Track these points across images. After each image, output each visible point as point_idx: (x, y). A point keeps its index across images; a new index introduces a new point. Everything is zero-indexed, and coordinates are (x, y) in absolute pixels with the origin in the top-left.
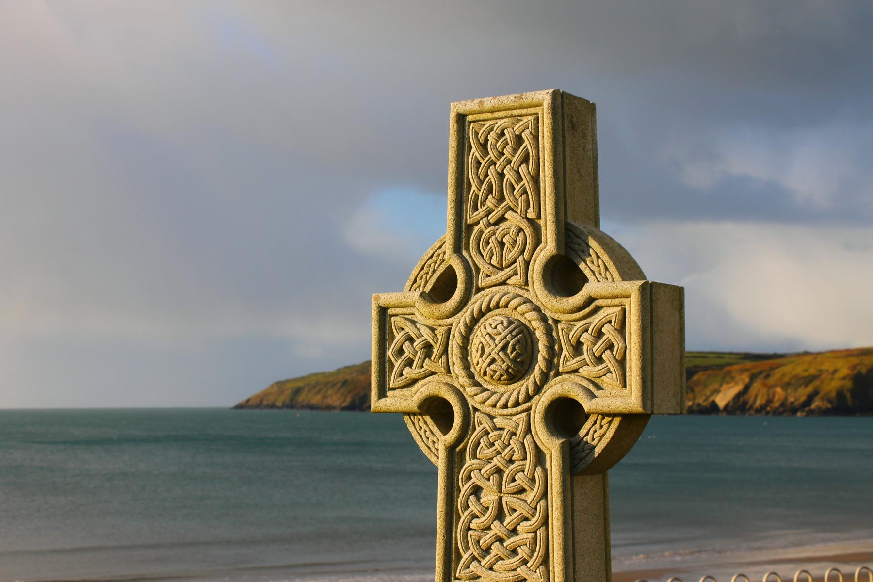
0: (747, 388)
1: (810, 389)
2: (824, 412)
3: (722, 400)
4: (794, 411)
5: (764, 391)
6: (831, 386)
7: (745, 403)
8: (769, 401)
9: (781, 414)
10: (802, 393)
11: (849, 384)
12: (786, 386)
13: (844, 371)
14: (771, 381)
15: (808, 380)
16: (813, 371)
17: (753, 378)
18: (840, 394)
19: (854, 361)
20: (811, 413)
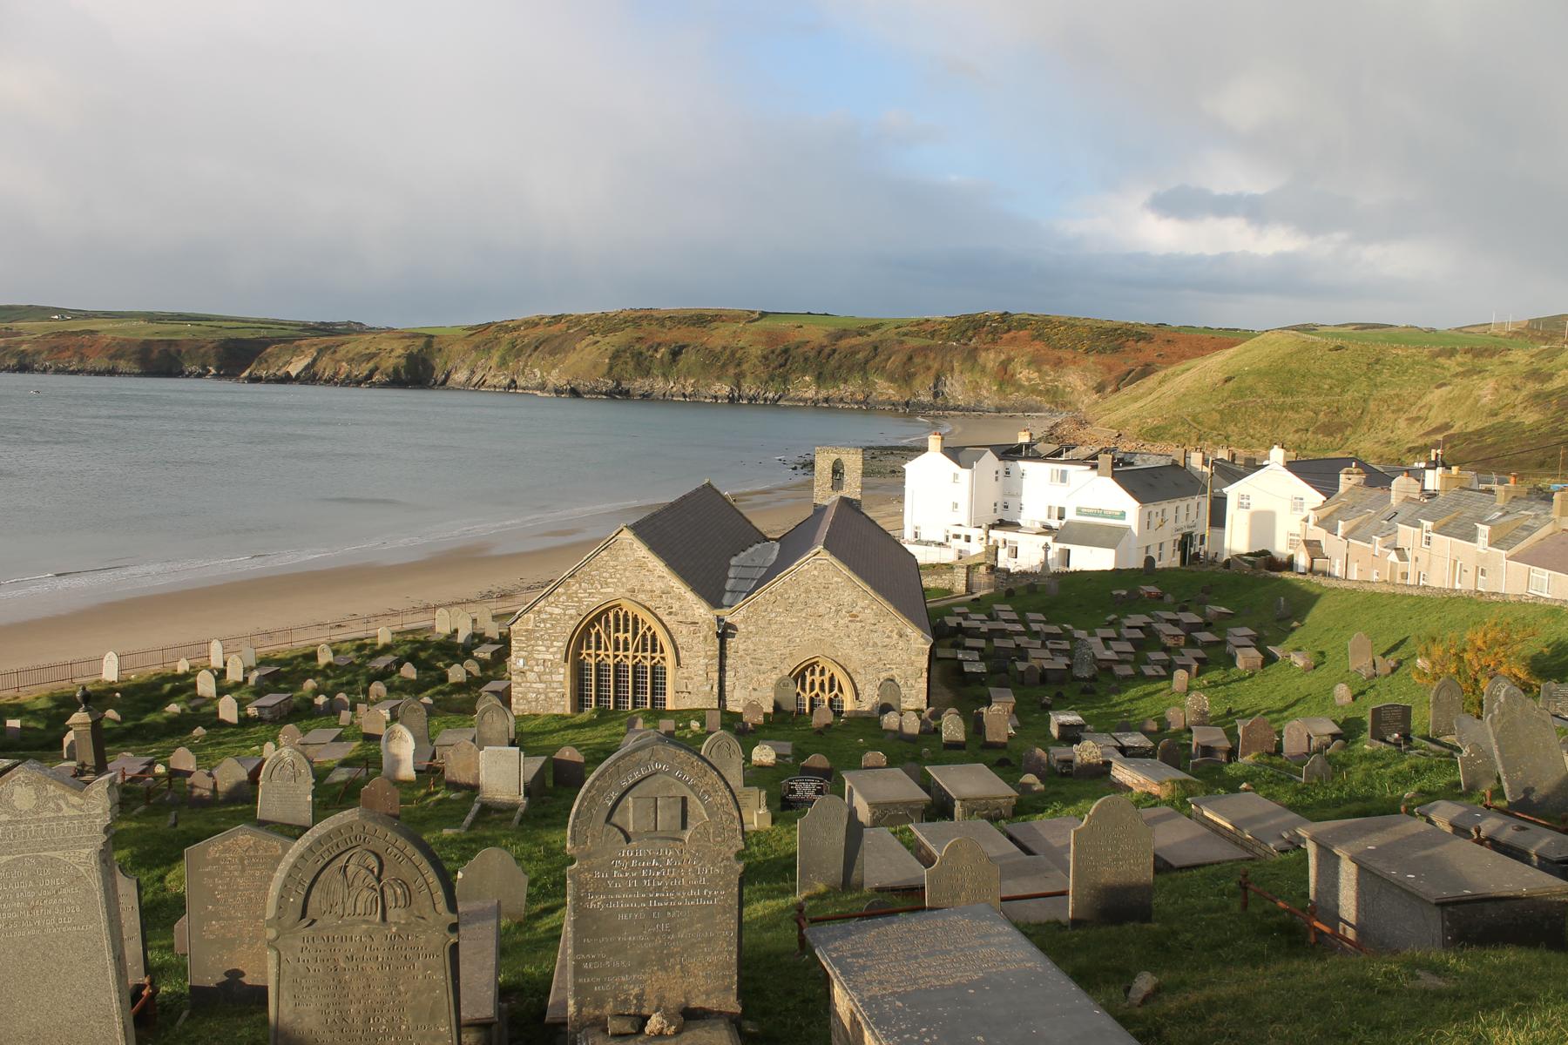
0: (315, 360)
1: (371, 365)
2: (384, 385)
3: (294, 369)
4: (358, 383)
5: (332, 364)
6: (389, 363)
7: (315, 374)
8: (336, 373)
9: (347, 385)
10: (365, 369)
11: (403, 361)
12: (350, 361)
13: (400, 351)
14: (338, 356)
15: (370, 357)
16: (373, 350)
17: (320, 352)
18: (396, 371)
19: (408, 342)
20: (373, 385)
